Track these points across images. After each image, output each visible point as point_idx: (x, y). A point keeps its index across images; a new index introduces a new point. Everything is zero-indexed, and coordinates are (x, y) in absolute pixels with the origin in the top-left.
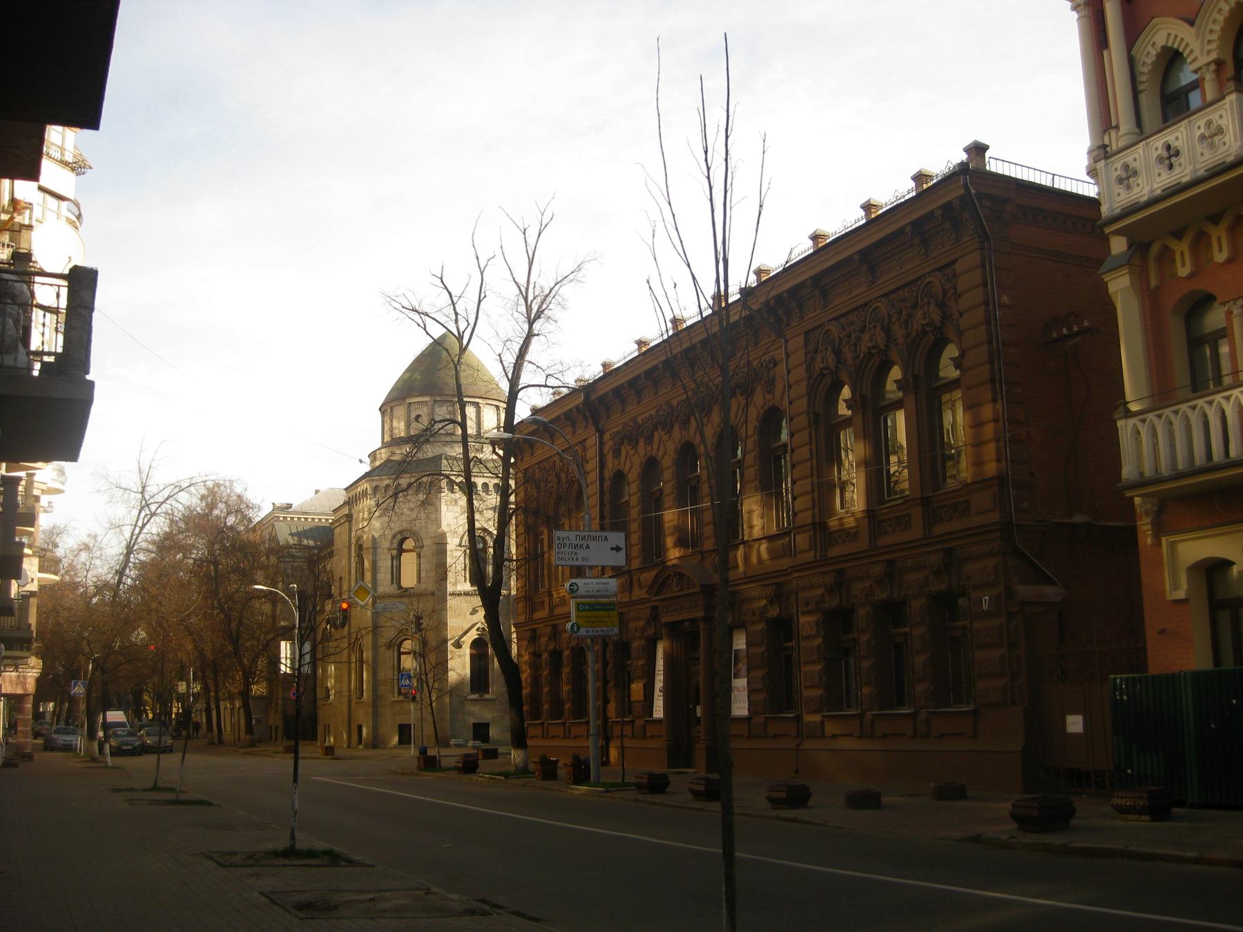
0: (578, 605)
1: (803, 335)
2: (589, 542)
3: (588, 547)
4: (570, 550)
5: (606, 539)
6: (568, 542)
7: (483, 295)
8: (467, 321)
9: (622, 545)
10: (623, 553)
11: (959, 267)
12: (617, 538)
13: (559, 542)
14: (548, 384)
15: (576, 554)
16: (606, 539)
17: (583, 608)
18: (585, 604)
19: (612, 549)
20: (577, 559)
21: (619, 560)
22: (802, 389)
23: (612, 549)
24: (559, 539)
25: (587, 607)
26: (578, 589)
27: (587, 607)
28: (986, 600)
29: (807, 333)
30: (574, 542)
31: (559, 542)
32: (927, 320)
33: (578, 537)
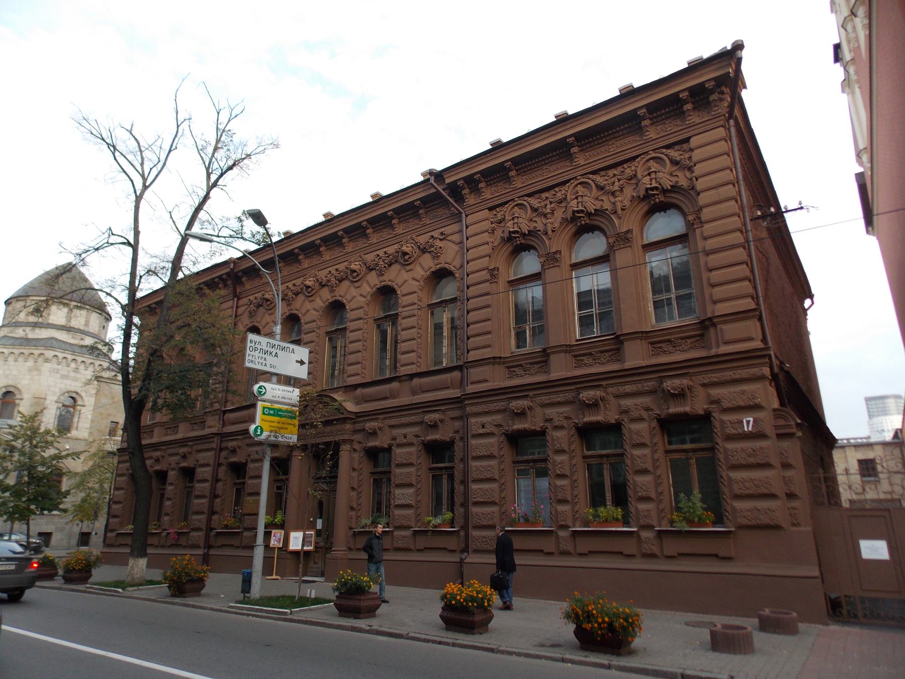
0: (264, 408)
2: (278, 351)
3: (276, 355)
4: (261, 355)
5: (293, 351)
6: (259, 347)
7: (174, 147)
8: (159, 159)
9: (306, 360)
10: (306, 367)
11: (694, 142)
12: (303, 353)
13: (251, 345)
14: (220, 235)
15: (265, 359)
16: (293, 351)
17: (267, 413)
18: (269, 409)
19: (297, 361)
20: (266, 365)
21: (302, 373)
23: (297, 361)
24: (251, 341)
25: (272, 412)
26: (265, 393)
27: (272, 412)
28: (748, 422)
29: (490, 209)
30: (264, 348)
31: (251, 345)
33: (269, 344)
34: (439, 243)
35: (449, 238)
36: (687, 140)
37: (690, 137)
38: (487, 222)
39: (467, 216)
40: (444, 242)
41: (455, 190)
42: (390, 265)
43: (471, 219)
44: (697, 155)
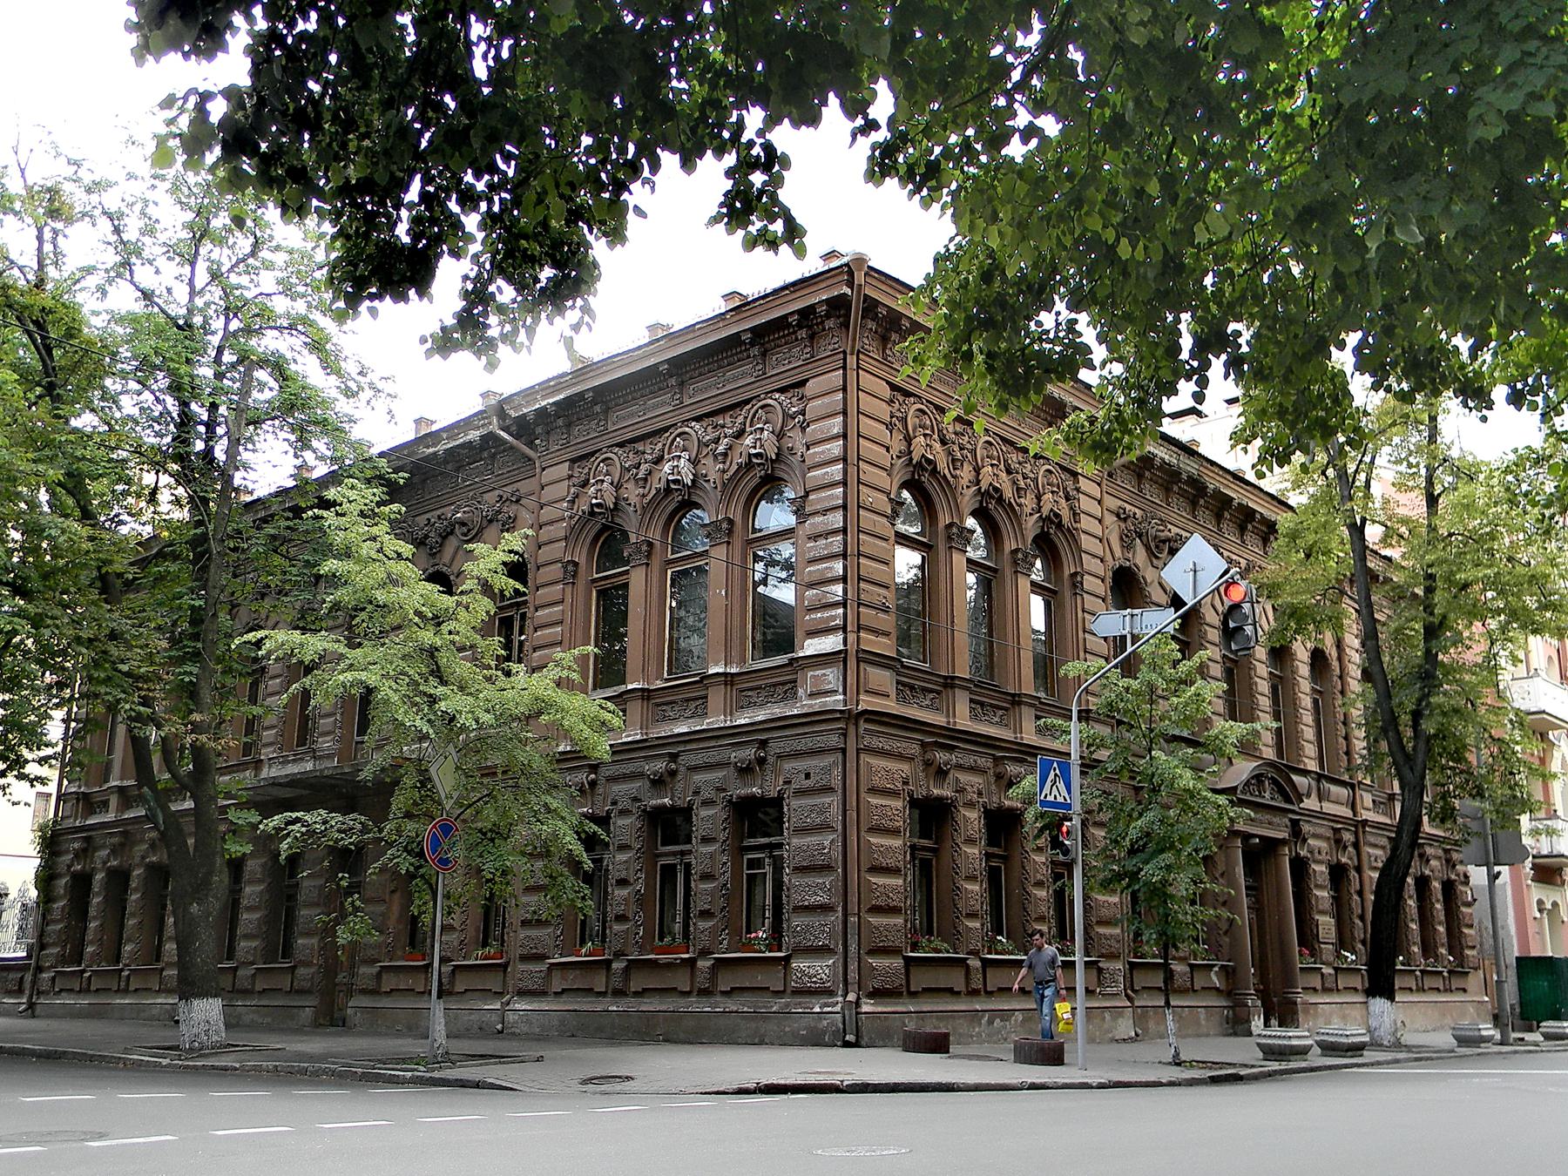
1: (567, 464)
11: (812, 387)
22: (560, 529)
29: (573, 461)
32: (758, 451)
34: (512, 510)
35: (523, 501)
36: (803, 383)
37: (807, 380)
38: (566, 482)
39: (544, 469)
40: (514, 507)
41: (524, 428)
42: (444, 538)
43: (549, 475)
44: (814, 407)
